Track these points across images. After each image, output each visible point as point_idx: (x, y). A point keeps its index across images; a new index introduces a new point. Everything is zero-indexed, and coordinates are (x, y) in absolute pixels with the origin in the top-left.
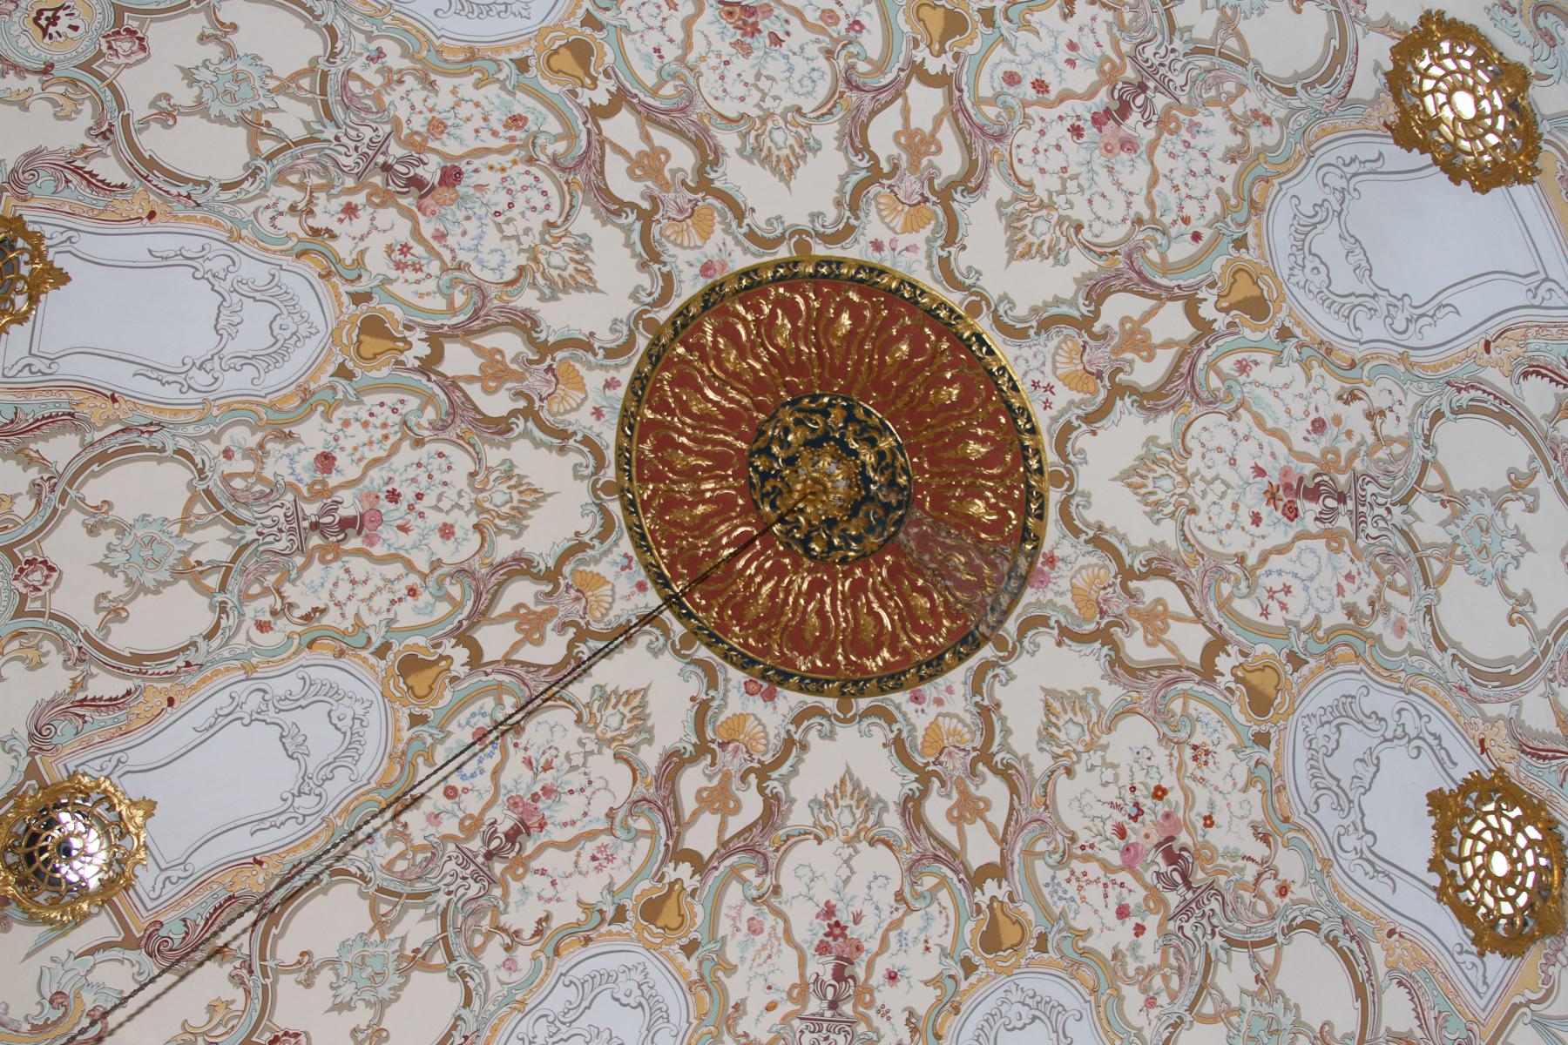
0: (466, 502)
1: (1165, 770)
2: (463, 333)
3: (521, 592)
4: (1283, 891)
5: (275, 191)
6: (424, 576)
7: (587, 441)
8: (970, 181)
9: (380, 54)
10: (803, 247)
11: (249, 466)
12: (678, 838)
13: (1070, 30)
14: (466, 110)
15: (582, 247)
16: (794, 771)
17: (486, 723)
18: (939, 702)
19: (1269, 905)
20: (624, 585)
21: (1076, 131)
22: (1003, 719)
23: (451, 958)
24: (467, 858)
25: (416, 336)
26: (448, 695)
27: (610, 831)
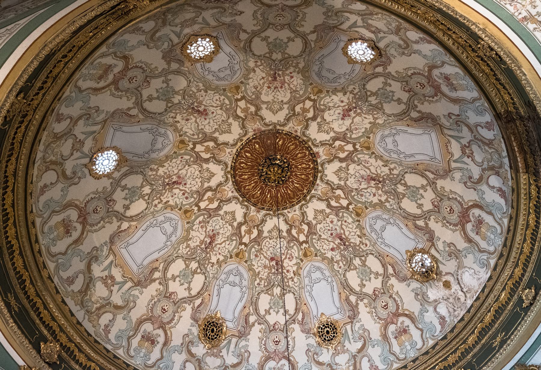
0: (325, 222)
1: (265, 90)
2: (297, 240)
3: (333, 203)
4: (256, 62)
5: (291, 286)
6: (342, 221)
7: (301, 209)
8: (210, 189)
9: (258, 284)
10: (243, 201)
11: (340, 263)
12: (353, 151)
13: (170, 199)
14: (260, 265)
15: (270, 232)
16: (326, 140)
17: (359, 196)
18: (293, 128)
19: (261, 61)
20: (320, 188)
21: (185, 184)
22: (286, 117)
23: (401, 179)
24: (383, 186)
25: (303, 247)
26: (359, 205)
27: (361, 163)
